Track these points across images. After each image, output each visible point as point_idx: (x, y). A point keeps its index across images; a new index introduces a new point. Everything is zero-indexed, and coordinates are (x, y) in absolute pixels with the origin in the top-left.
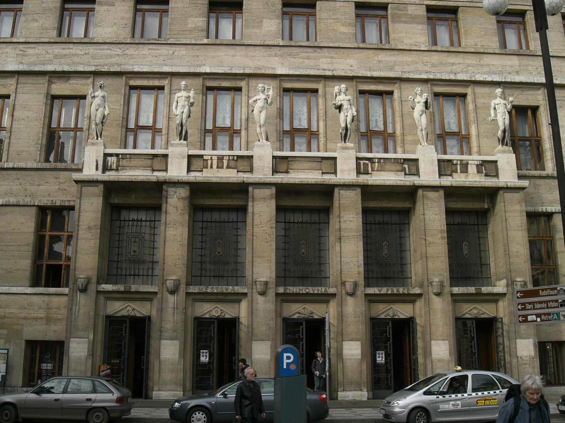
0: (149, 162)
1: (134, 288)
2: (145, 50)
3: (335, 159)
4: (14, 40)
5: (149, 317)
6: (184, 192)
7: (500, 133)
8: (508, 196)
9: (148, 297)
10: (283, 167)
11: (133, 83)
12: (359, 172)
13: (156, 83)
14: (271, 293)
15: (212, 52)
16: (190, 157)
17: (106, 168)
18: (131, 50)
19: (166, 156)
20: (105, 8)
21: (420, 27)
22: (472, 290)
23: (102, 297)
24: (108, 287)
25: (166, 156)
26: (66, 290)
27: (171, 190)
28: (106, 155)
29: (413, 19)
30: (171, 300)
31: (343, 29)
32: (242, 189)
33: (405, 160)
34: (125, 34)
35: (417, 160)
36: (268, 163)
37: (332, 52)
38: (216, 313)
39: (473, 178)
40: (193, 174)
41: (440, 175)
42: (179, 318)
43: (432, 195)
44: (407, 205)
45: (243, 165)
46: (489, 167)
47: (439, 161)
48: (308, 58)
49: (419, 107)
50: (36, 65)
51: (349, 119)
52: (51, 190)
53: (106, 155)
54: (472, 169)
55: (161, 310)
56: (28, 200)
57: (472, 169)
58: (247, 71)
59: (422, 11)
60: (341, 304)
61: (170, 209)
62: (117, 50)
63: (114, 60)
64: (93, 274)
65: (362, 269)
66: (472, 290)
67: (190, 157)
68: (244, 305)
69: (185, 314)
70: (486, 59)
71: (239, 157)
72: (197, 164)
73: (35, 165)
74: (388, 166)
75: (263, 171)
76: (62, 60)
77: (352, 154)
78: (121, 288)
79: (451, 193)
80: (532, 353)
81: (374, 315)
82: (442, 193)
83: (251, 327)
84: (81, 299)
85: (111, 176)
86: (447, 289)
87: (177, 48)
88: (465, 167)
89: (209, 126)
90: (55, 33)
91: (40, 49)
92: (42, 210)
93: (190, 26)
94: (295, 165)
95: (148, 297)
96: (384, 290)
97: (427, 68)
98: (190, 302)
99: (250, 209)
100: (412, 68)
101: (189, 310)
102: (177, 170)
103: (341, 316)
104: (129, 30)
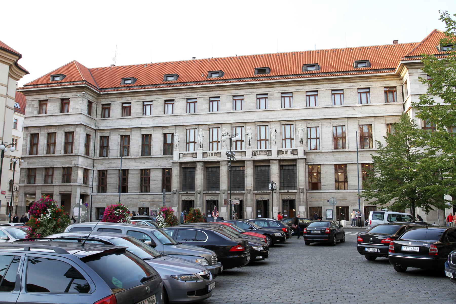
0: (192, 155)
2: (190, 117)
4: (151, 116)
5: (193, 201)
6: (201, 164)
7: (300, 140)
8: (300, 161)
9: (193, 195)
11: (187, 128)
12: (252, 155)
13: (194, 127)
14: (226, 193)
15: (210, 116)
16: (203, 153)
17: (180, 158)
18: (186, 117)
19: (196, 153)
20: (177, 103)
21: (278, 101)
22: (286, 191)
23: (180, 195)
25: (196, 153)
26: (170, 193)
27: (198, 164)
28: (180, 154)
29: (276, 98)
30: (199, 195)
31: (252, 105)
34: (184, 112)
35: (271, 151)
37: (248, 113)
38: (212, 199)
39: (290, 156)
41: (278, 154)
42: (201, 200)
43: (275, 162)
44: (269, 164)
45: (218, 155)
46: (294, 152)
48: (240, 116)
49: (273, 132)
50: (158, 124)
51: (251, 138)
52: (165, 164)
53: (180, 154)
54: (289, 152)
55: (196, 198)
56: (159, 167)
57: (289, 152)
58: (221, 122)
59: (279, 95)
60: (246, 196)
61: (198, 169)
62: (181, 117)
63: (181, 121)
65: (252, 186)
66: (286, 191)
67: (203, 153)
68: (219, 196)
69: (203, 199)
70: (301, 111)
72: (205, 155)
73: (160, 156)
74: (262, 153)
75: (224, 157)
77: (251, 150)
78: (185, 192)
80: (304, 210)
81: (257, 199)
82: (278, 161)
83: (221, 203)
84: (175, 196)
85: (181, 160)
86: (278, 191)
87: (200, 116)
88: (286, 152)
89: (211, 141)
90: (163, 113)
91: (159, 119)
92: (164, 169)
93: (204, 107)
95: (193, 195)
96: (259, 192)
97: (280, 116)
98: (204, 196)
99: (220, 168)
100: (275, 117)
101: (204, 199)
102: (200, 158)
103: (246, 199)
104: (185, 110)
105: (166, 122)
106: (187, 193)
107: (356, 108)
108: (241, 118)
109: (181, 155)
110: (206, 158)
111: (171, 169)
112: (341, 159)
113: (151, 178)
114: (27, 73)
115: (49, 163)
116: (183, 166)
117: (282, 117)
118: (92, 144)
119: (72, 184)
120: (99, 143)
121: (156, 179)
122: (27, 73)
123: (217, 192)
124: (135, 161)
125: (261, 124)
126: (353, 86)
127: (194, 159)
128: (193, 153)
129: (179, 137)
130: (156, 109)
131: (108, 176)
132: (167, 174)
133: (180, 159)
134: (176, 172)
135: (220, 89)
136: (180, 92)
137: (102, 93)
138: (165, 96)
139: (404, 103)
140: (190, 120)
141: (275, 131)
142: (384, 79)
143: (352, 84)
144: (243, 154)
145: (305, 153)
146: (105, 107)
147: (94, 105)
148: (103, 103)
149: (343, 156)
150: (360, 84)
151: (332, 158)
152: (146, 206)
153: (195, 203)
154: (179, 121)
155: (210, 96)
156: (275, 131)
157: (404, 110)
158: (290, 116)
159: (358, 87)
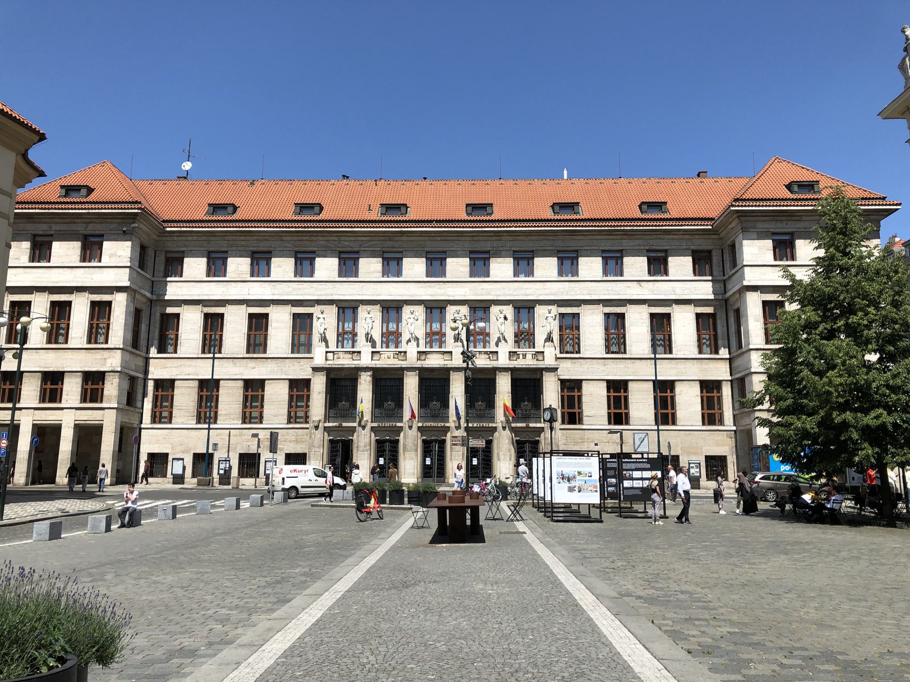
1: (344, 424)
3: (451, 352)
10: (423, 357)
17: (326, 359)
22: (524, 425)
24: (331, 424)
28: (327, 352)
31: (462, 269)
32: (402, 370)
33: (491, 352)
35: (497, 352)
36: (415, 355)
40: (373, 362)
45: (401, 357)
47: (510, 352)
53: (327, 352)
54: (529, 356)
57: (529, 356)
63: (328, 292)
64: (322, 417)
66: (524, 425)
67: (373, 352)
71: (400, 352)
72: (376, 357)
76: (298, 292)
79: (513, 370)
88: (524, 356)
93: (372, 269)
94: (429, 356)
97: (510, 292)
105: (298, 292)
106: (340, 426)
107: (643, 284)
108: (440, 291)
109: (330, 356)
110: (377, 362)
111: (310, 380)
112: (617, 371)
113: (266, 397)
114: (42, 174)
115: (53, 361)
116: (332, 376)
117: (515, 293)
118: (143, 327)
119: (104, 405)
120: (158, 325)
121: (276, 398)
122: (42, 174)
123: (399, 424)
124: (235, 364)
125: (478, 306)
126: (639, 245)
127: (355, 362)
128: (354, 352)
129: (325, 321)
130: (279, 266)
131: (176, 391)
132: (299, 389)
133: (329, 362)
134: (319, 385)
135: (404, 238)
136: (328, 238)
137: (168, 229)
138: (298, 243)
139: (725, 278)
140: (348, 291)
141: (505, 318)
142: (692, 237)
143: (638, 242)
144: (447, 357)
145: (557, 358)
146: (169, 255)
147: (150, 253)
148: (168, 249)
149: (621, 365)
150: (651, 242)
151: (603, 368)
152: (253, 450)
153: (355, 446)
154: (324, 292)
155: (384, 249)
156: (505, 318)
157: (725, 292)
158: (529, 292)
159: (647, 248)
